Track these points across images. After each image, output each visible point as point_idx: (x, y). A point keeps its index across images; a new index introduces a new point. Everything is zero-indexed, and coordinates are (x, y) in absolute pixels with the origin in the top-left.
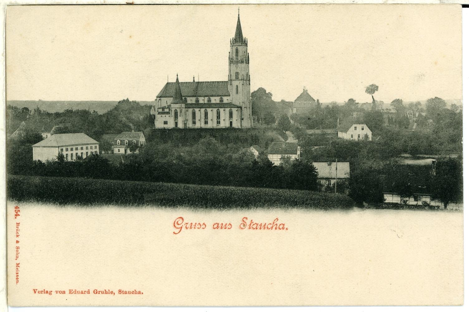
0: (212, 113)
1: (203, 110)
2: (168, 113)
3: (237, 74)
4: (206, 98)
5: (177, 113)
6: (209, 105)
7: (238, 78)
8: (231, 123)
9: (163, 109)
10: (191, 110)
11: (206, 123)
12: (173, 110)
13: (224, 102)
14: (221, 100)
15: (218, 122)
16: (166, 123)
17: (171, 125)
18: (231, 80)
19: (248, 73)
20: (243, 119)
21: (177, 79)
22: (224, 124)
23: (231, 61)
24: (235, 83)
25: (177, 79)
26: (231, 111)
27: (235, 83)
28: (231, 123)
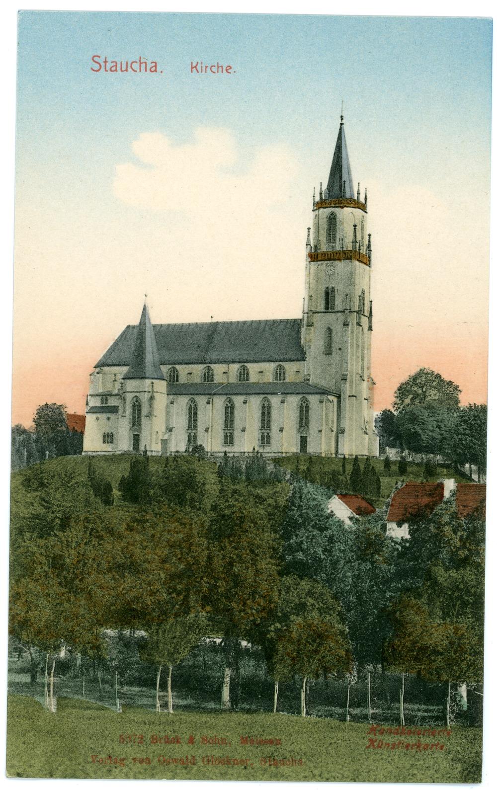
1: (219, 402)
2: (114, 410)
4: (235, 367)
5: (140, 406)
6: (244, 387)
7: (333, 308)
8: (304, 442)
10: (183, 401)
12: (129, 397)
13: (287, 380)
14: (280, 374)
15: (263, 437)
17: (124, 444)
18: (311, 312)
19: (366, 294)
20: (343, 432)
22: (286, 442)
23: (315, 256)
24: (322, 321)
26: (304, 405)
28: (304, 442)
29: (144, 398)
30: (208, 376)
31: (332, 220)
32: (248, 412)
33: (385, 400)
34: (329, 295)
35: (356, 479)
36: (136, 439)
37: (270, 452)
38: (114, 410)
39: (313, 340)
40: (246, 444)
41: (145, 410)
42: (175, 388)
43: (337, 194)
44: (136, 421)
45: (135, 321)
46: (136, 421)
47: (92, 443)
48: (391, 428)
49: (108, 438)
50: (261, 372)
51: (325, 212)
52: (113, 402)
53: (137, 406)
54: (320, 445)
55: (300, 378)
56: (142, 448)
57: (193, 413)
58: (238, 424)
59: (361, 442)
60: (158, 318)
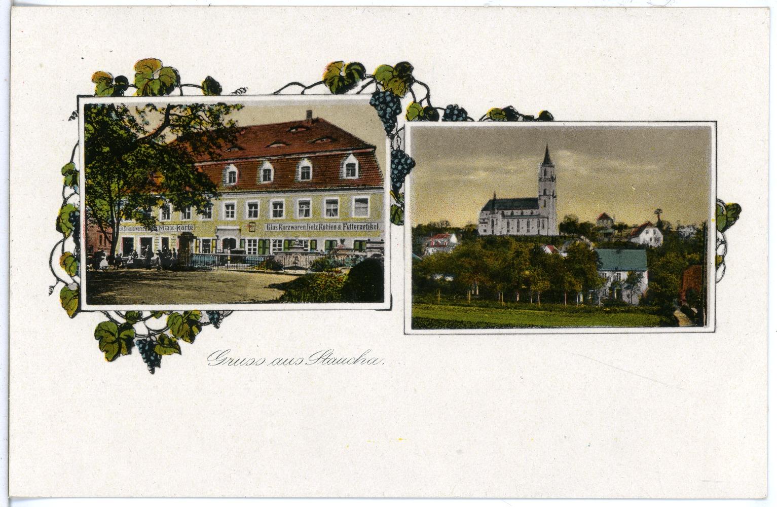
0: (523, 223)
1: (516, 221)
2: (487, 223)
3: (545, 191)
9: (484, 219)
10: (506, 220)
11: (518, 231)
12: (491, 219)
16: (485, 231)
17: (489, 233)
18: (540, 196)
21: (495, 196)
22: (534, 232)
24: (543, 198)
25: (495, 196)
27: (543, 198)
29: (495, 220)
30: (512, 213)
31: (545, 172)
32: (523, 223)
33: (561, 219)
34: (545, 191)
35: (553, 241)
36: (493, 231)
37: (529, 234)
38: (487, 223)
39: (541, 203)
40: (523, 232)
41: (495, 223)
42: (504, 216)
43: (547, 161)
44: (493, 226)
45: (492, 198)
46: (493, 226)
47: (481, 233)
48: (562, 227)
49: (485, 231)
50: (527, 212)
51: (544, 168)
52: (486, 221)
53: (493, 222)
54: (543, 233)
55: (537, 214)
56: (494, 234)
57: (508, 223)
58: (521, 227)
59: (554, 231)
60: (498, 197)
